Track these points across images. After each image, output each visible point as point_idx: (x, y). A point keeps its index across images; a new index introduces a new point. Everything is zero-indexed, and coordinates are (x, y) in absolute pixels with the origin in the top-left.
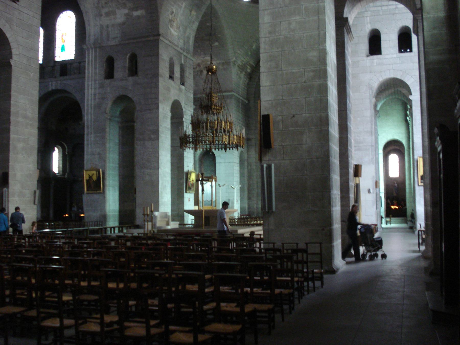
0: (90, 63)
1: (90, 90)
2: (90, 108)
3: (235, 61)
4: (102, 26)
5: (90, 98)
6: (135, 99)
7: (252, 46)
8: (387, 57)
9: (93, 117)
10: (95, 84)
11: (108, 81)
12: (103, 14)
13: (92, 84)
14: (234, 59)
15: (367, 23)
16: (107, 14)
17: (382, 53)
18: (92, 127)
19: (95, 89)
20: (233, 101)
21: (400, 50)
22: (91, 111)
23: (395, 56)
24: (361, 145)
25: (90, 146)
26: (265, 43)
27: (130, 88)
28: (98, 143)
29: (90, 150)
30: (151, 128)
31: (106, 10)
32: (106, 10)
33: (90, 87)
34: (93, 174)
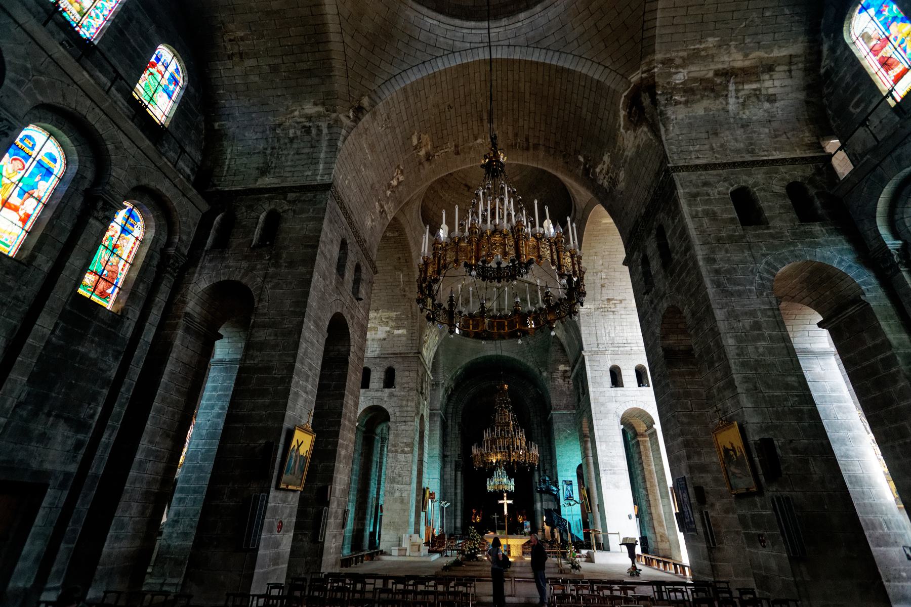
6: (390, 411)
8: (628, 389)
20: (439, 419)
26: (735, 363)
27: (385, 399)
30: (405, 441)
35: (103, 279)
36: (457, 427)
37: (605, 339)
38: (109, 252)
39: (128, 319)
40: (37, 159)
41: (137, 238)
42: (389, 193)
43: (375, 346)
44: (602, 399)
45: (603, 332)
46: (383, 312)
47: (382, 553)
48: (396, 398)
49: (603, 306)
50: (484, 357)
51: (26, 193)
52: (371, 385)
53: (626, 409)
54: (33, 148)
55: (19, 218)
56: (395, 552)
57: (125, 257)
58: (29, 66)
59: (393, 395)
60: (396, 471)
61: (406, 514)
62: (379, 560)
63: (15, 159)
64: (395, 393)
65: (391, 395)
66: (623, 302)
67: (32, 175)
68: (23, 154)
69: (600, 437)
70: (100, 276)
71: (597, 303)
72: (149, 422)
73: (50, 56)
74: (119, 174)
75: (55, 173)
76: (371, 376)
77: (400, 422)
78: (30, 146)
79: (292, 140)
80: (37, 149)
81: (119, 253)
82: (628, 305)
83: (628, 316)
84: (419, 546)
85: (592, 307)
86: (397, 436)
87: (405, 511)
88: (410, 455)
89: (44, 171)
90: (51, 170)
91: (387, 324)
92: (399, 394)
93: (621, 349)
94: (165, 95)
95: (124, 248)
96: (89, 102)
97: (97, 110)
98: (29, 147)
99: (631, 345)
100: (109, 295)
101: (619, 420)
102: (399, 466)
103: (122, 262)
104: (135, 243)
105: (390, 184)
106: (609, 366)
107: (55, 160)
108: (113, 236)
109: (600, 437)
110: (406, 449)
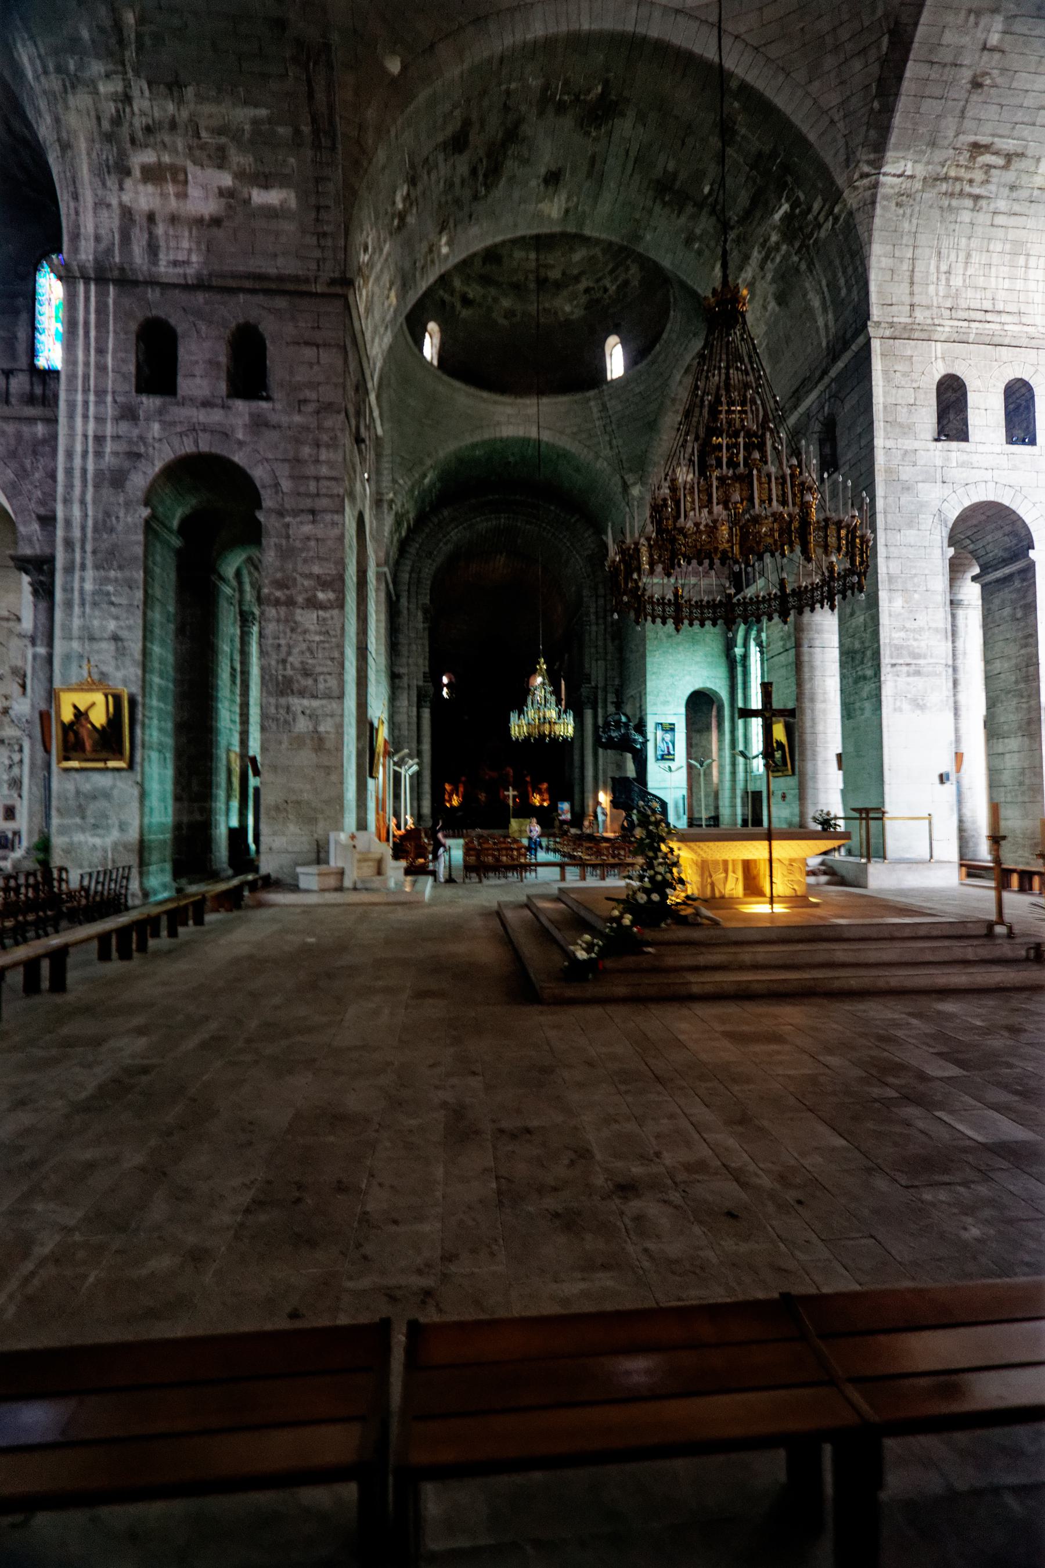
0: (81, 332)
1: (79, 421)
2: (77, 482)
3: (392, 501)
4: (127, 213)
5: (79, 448)
6: (259, 474)
7: (425, 476)
8: (981, 448)
9: (90, 513)
10: (100, 401)
11: (150, 403)
12: (137, 173)
13: (86, 403)
14: (391, 495)
15: (936, 359)
16: (152, 175)
17: (970, 439)
18: (89, 548)
19: (100, 420)
21: (1011, 440)
22: (84, 493)
23: (998, 449)
24: (921, 662)
25: (77, 610)
27: (240, 436)
28: (112, 604)
29: (76, 623)
30: (316, 569)
31: (147, 157)
32: (147, 157)
33: (79, 410)
34: (93, 704)
36: (420, 614)
37: (933, 293)
43: (185, 244)
44: (906, 473)
45: (933, 269)
46: (200, 98)
47: (269, 883)
48: (273, 436)
49: (952, 173)
50: (494, 441)
52: (185, 386)
53: (967, 503)
56: (309, 878)
59: (267, 425)
60: (294, 659)
61: (334, 778)
62: (261, 905)
64: (274, 418)
65: (259, 424)
66: (1017, 164)
69: (891, 578)
71: (939, 155)
76: (182, 352)
77: (296, 513)
82: (1025, 179)
83: (1013, 221)
84: (380, 862)
85: (920, 171)
86: (286, 553)
87: (328, 770)
88: (335, 612)
91: (220, 161)
92: (284, 420)
93: (974, 325)
99: (1005, 318)
101: (945, 533)
102: (304, 646)
106: (937, 377)
109: (891, 578)
110: (321, 595)
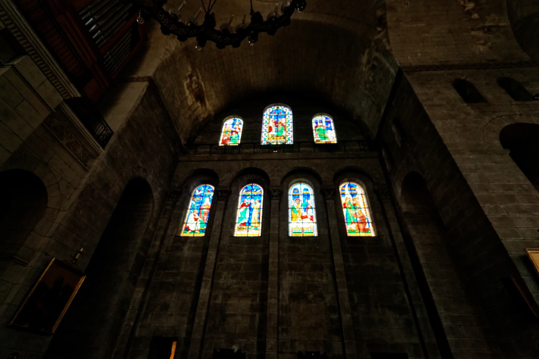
35: (360, 223)
38: (353, 209)
39: (383, 235)
40: (302, 194)
41: (362, 194)
42: (476, 16)
51: (306, 209)
54: (298, 192)
55: (309, 219)
57: (362, 206)
58: (273, 168)
63: (296, 200)
67: (304, 201)
68: (297, 196)
70: (357, 222)
72: (433, 295)
73: (276, 159)
74: (326, 175)
75: (310, 194)
78: (297, 191)
79: (374, 81)
80: (299, 191)
81: (358, 206)
89: (307, 197)
90: (309, 194)
94: (329, 131)
95: (359, 203)
96: (296, 161)
97: (300, 160)
98: (297, 193)
100: (368, 229)
103: (363, 210)
104: (362, 197)
105: (469, 13)
107: (307, 190)
108: (350, 201)
